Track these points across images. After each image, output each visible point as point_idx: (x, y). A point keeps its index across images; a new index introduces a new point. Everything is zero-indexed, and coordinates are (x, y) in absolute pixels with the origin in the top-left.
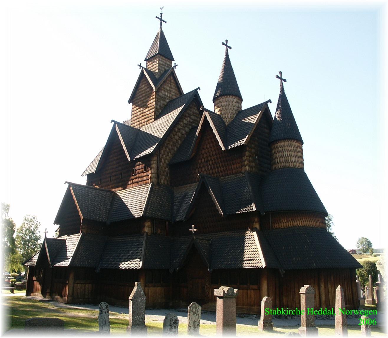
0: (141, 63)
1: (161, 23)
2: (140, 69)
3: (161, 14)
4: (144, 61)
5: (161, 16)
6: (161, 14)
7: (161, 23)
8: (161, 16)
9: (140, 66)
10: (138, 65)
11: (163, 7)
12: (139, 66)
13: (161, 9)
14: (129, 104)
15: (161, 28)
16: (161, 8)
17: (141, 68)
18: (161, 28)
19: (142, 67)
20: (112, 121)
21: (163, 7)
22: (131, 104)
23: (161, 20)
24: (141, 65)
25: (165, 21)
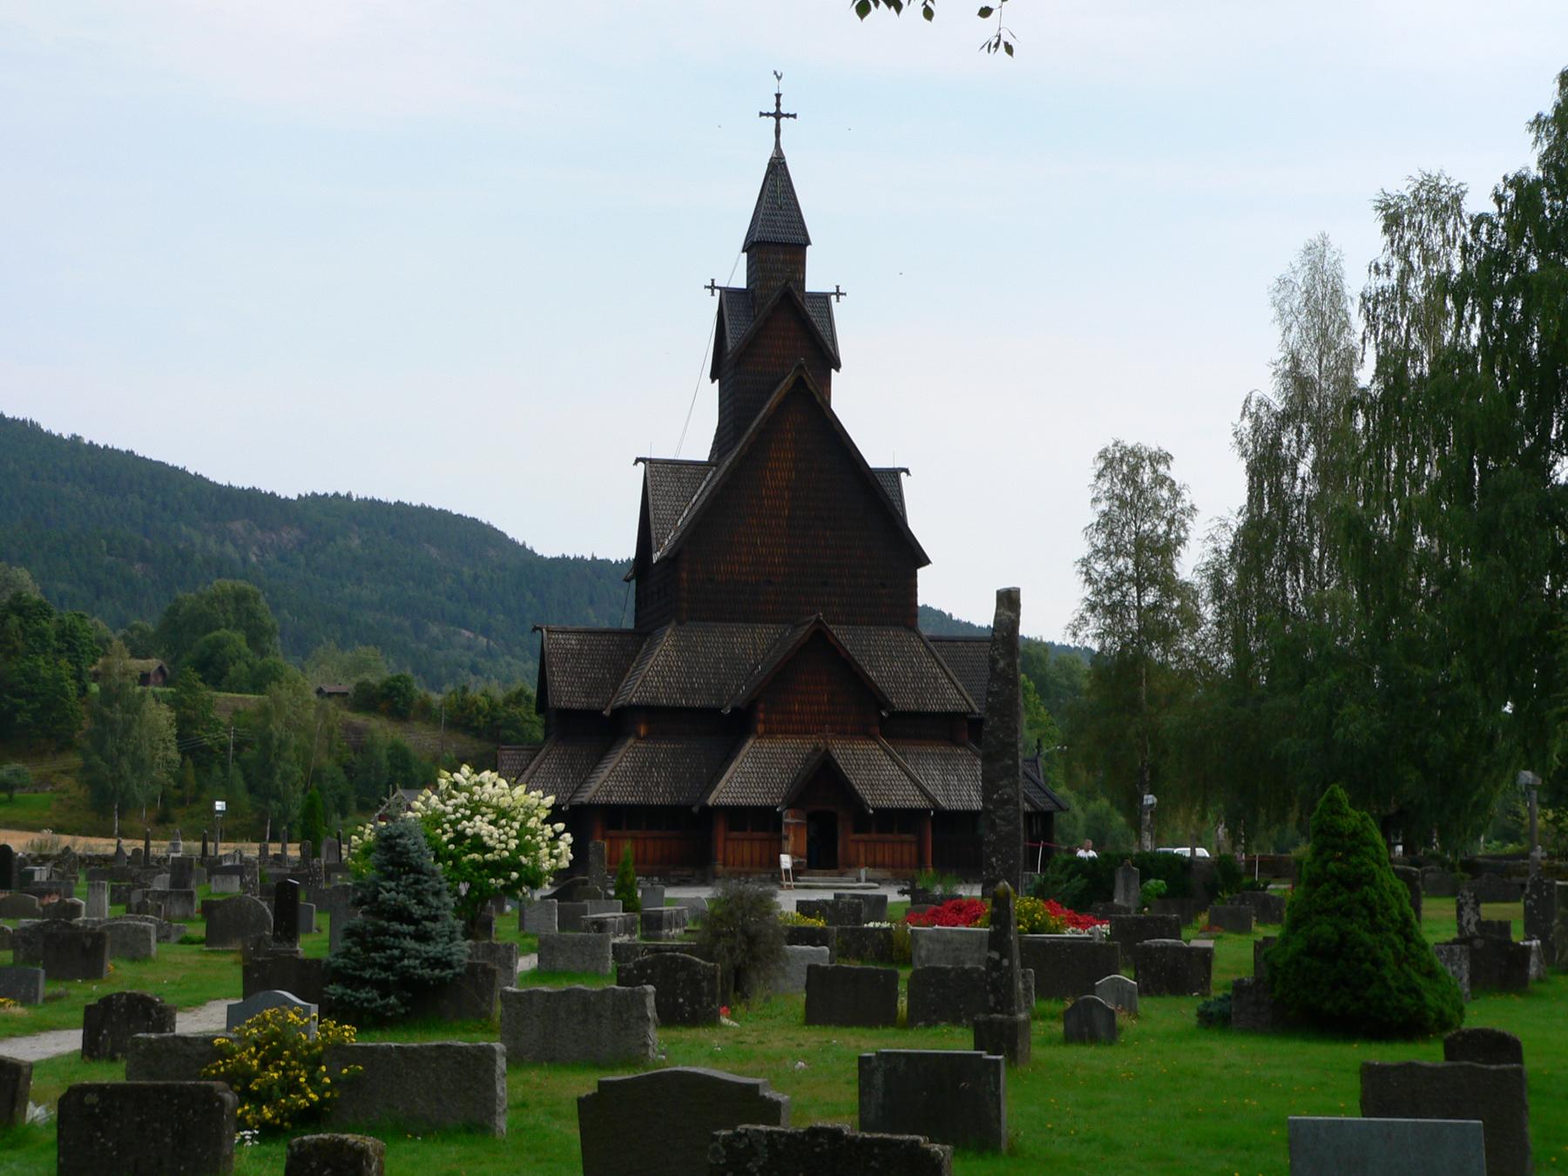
0: (713, 280)
1: (778, 125)
2: (713, 294)
3: (778, 96)
4: (743, 251)
5: (778, 105)
6: (778, 96)
7: (778, 125)
8: (778, 105)
9: (713, 287)
14: (713, 381)
17: (717, 292)
19: (718, 288)
20: (638, 460)
22: (717, 381)
23: (778, 115)
25: (791, 113)
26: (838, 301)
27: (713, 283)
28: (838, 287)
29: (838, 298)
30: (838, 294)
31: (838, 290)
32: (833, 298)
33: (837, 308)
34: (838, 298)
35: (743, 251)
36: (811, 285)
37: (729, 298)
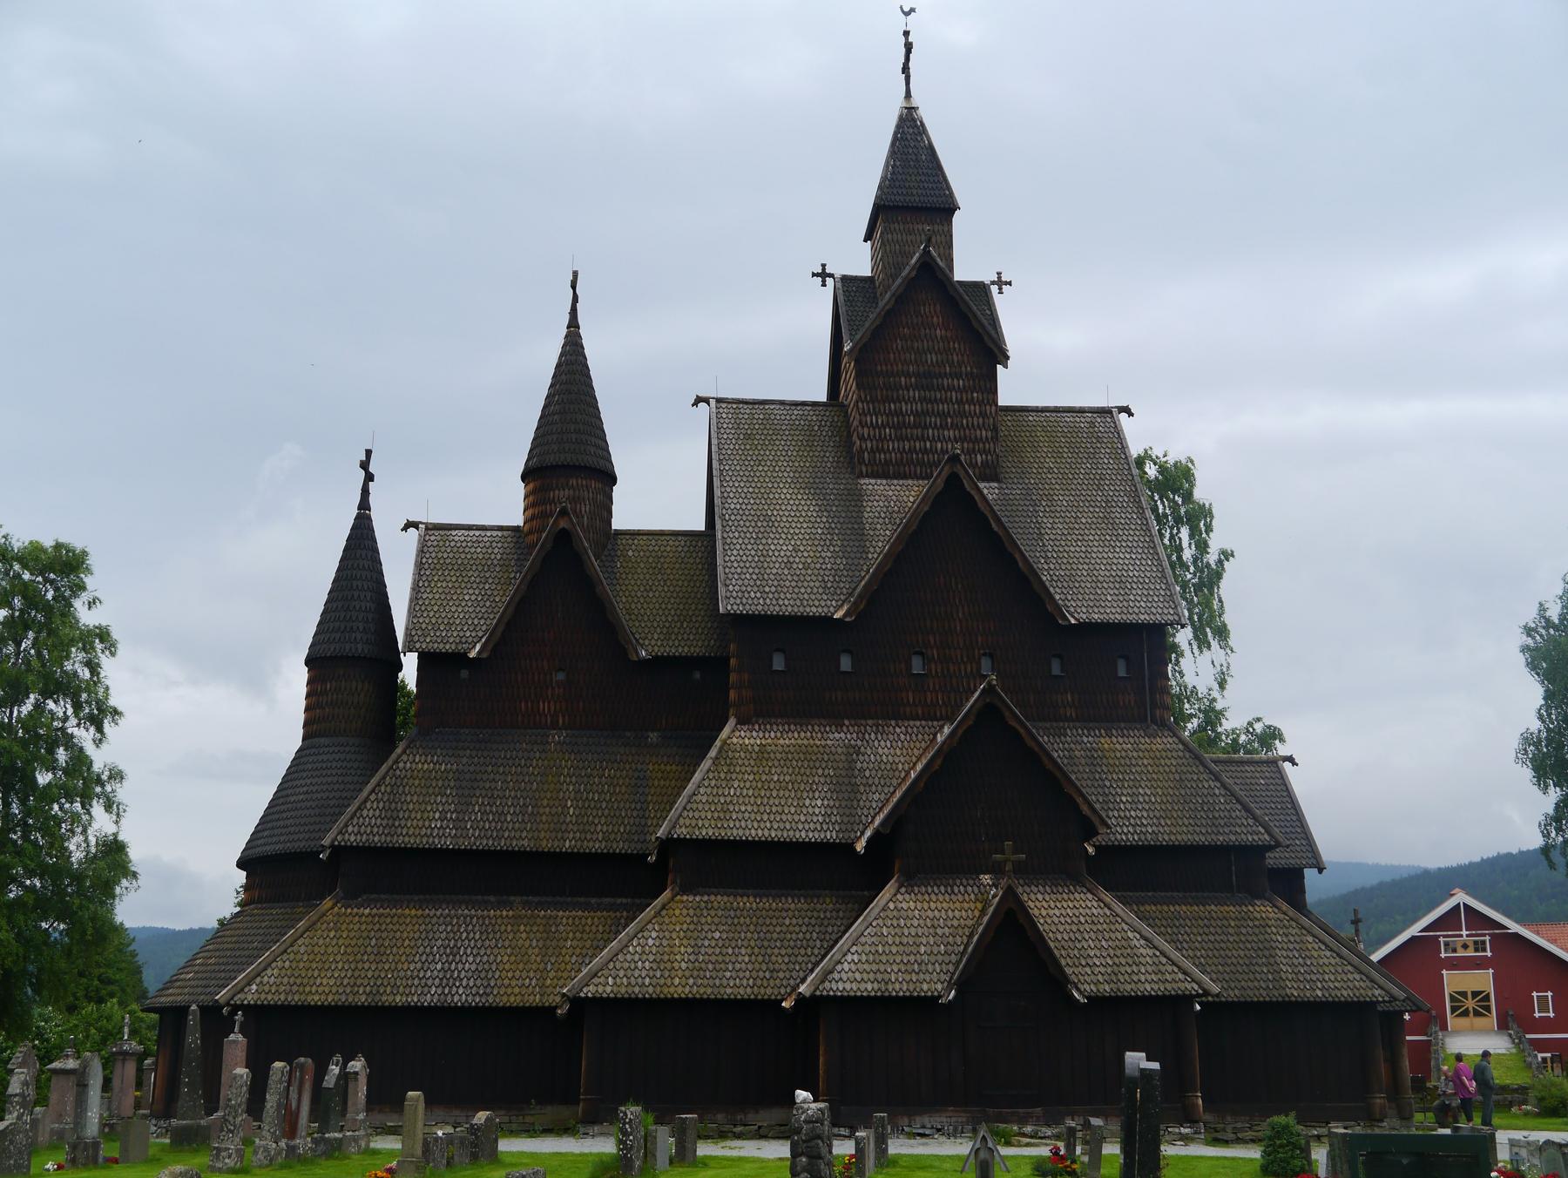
0: (824, 266)
2: (824, 285)
3: (906, 34)
4: (865, 241)
9: (823, 275)
10: (814, 275)
11: (912, 10)
12: (820, 279)
13: (907, 14)
15: (908, 95)
16: (906, 9)
18: (908, 95)
19: (831, 276)
21: (912, 10)
24: (828, 271)
26: (1001, 292)
27: (824, 269)
28: (999, 274)
29: (1000, 289)
30: (1000, 283)
31: (999, 278)
32: (994, 289)
33: (1004, 305)
34: (1000, 289)
35: (865, 241)
36: (963, 271)
37: (851, 292)
